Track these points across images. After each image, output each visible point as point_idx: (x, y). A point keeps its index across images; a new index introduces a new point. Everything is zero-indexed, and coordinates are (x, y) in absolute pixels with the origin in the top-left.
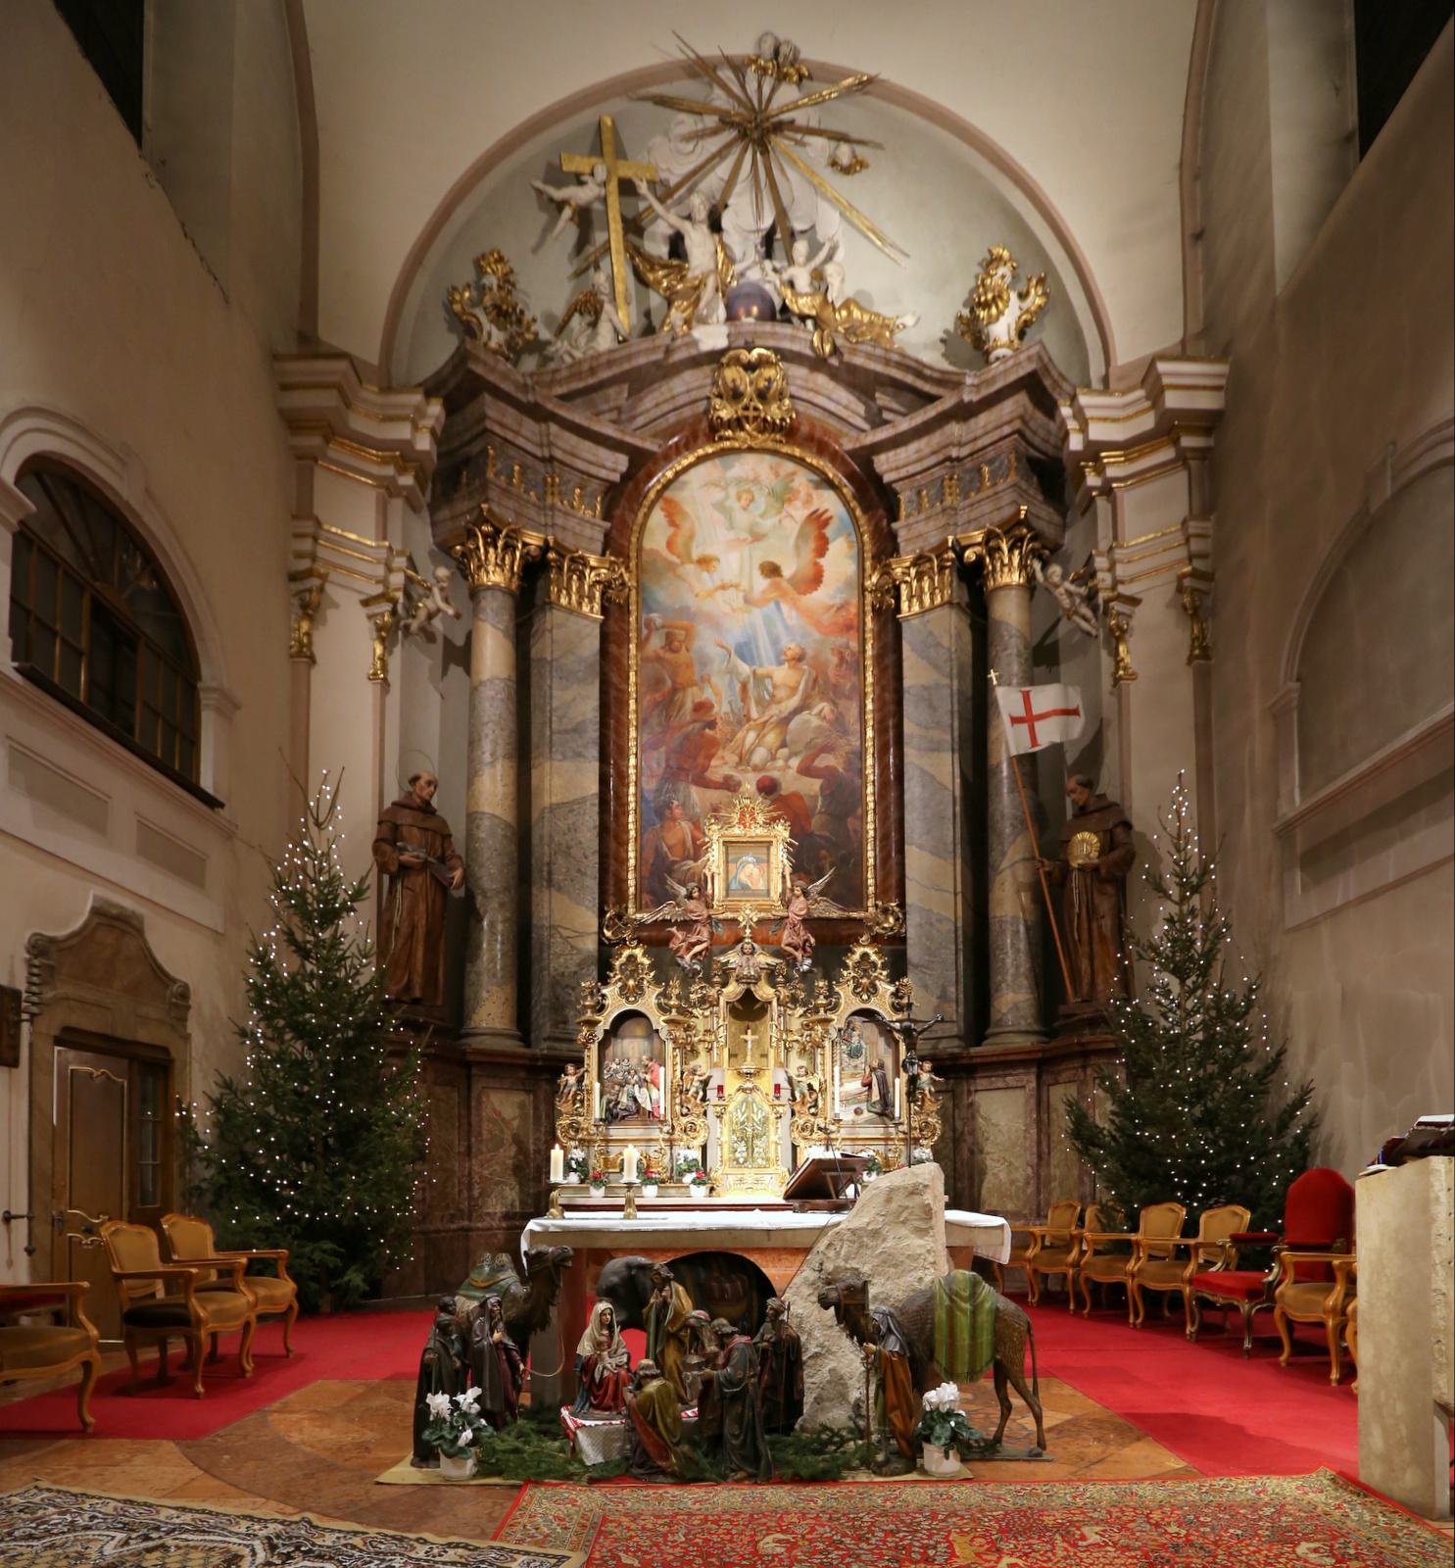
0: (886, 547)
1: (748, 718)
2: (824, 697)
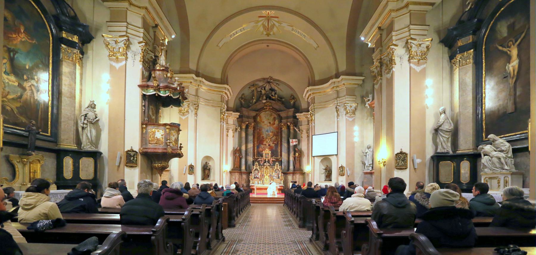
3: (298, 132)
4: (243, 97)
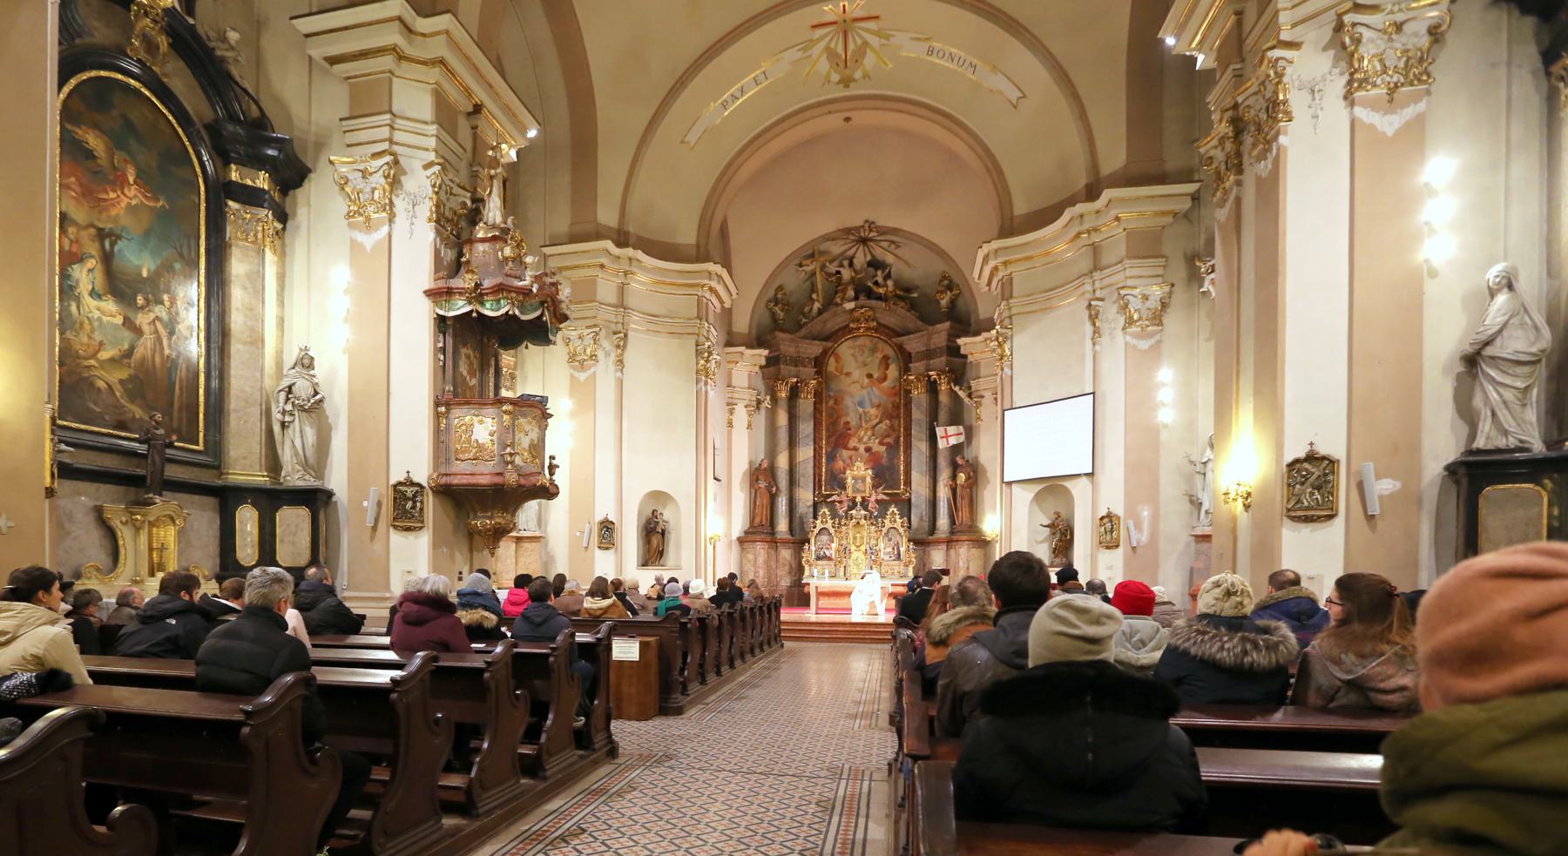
0: (906, 370)
2: (887, 418)
3: (967, 400)
4: (780, 296)
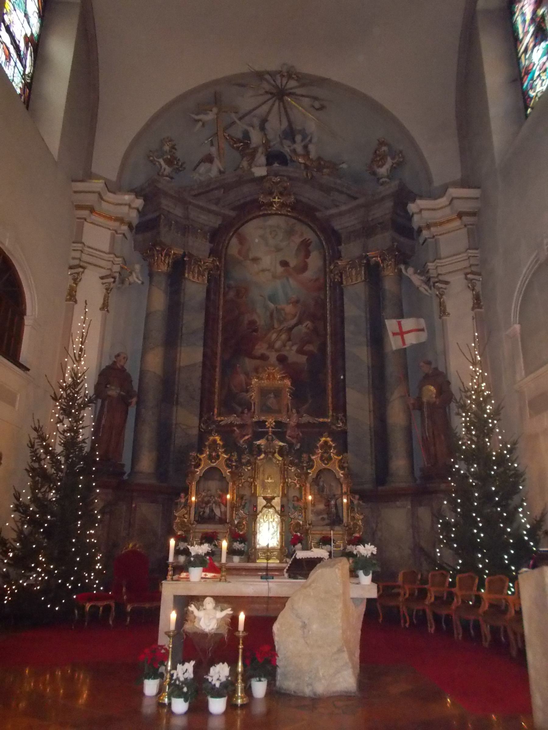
1: (274, 328)
3: (423, 288)
